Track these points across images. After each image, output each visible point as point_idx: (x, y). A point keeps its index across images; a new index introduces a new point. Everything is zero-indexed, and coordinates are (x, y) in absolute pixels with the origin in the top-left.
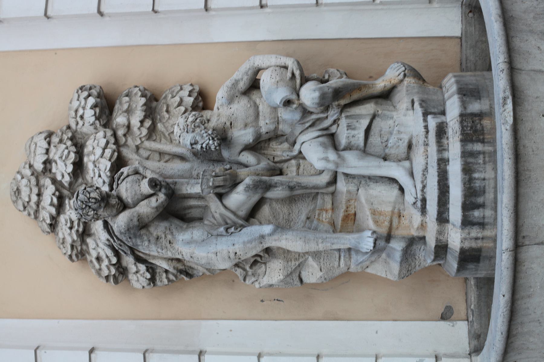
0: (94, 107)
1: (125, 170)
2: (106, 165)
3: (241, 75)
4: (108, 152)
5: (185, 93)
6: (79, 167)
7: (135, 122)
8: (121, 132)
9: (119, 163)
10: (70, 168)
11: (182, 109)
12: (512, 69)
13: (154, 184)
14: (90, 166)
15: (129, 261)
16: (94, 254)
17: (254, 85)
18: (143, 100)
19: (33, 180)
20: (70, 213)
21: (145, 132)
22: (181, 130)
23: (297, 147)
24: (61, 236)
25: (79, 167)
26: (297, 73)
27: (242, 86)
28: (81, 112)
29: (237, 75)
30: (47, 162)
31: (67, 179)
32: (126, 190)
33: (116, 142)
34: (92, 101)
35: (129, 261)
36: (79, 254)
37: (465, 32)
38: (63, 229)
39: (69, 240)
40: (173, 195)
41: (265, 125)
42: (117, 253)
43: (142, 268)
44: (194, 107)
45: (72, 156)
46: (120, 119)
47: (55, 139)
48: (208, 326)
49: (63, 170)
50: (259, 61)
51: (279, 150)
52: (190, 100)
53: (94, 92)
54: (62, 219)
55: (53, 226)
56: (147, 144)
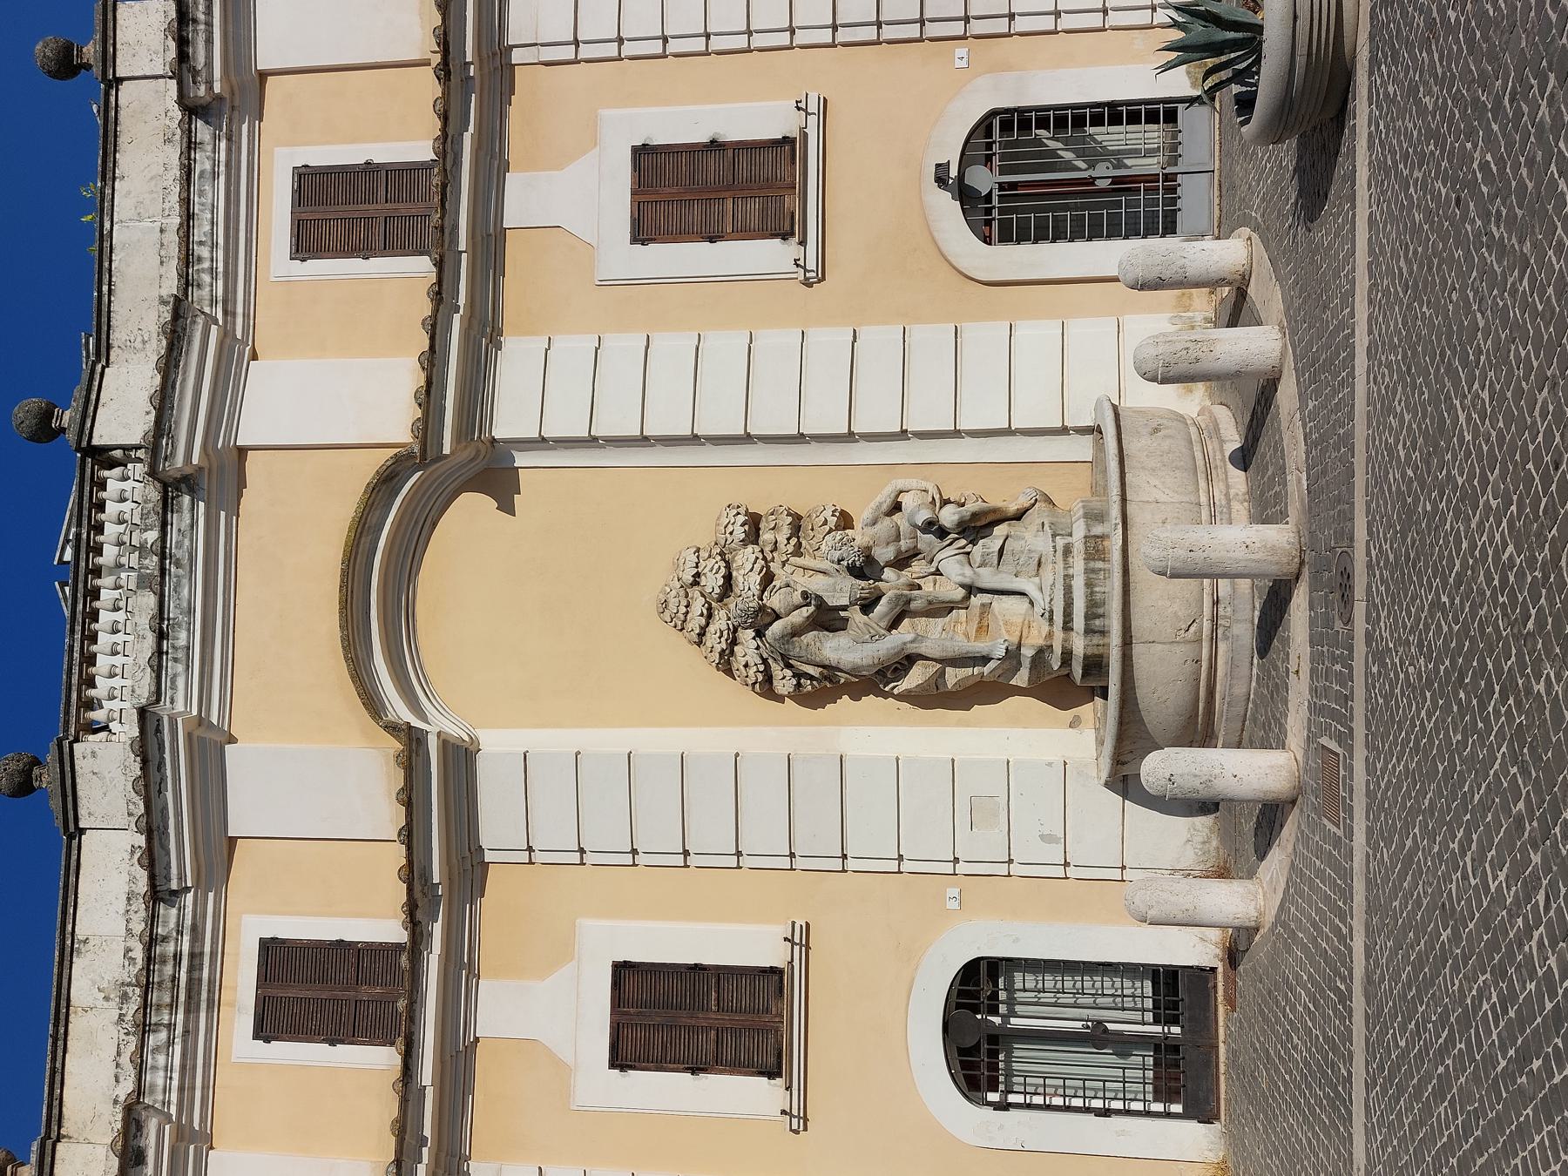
0: (743, 525)
1: (776, 583)
2: (755, 579)
3: (884, 497)
4: (757, 567)
5: (828, 513)
6: (728, 578)
7: (782, 539)
8: (767, 549)
9: (768, 579)
10: (721, 582)
11: (827, 528)
12: (1124, 500)
13: (805, 595)
14: (741, 579)
15: (777, 670)
16: (743, 661)
17: (897, 507)
18: (790, 519)
19: (682, 593)
20: (720, 622)
21: (790, 548)
22: (827, 547)
23: (934, 564)
24: (709, 644)
25: (728, 578)
26: (937, 497)
27: (885, 507)
28: (730, 528)
29: (878, 499)
30: (698, 575)
31: (717, 590)
32: (775, 601)
33: (764, 558)
34: (741, 519)
35: (777, 670)
36: (726, 665)
37: (1095, 456)
38: (711, 639)
39: (718, 648)
40: (821, 604)
41: (905, 544)
42: (765, 661)
43: (788, 673)
44: (838, 528)
45: (723, 571)
46: (766, 536)
47: (703, 554)
48: (846, 731)
49: (713, 582)
50: (901, 483)
51: (918, 567)
52: (833, 521)
53: (743, 510)
54: (711, 628)
55: (702, 634)
56: (793, 560)
